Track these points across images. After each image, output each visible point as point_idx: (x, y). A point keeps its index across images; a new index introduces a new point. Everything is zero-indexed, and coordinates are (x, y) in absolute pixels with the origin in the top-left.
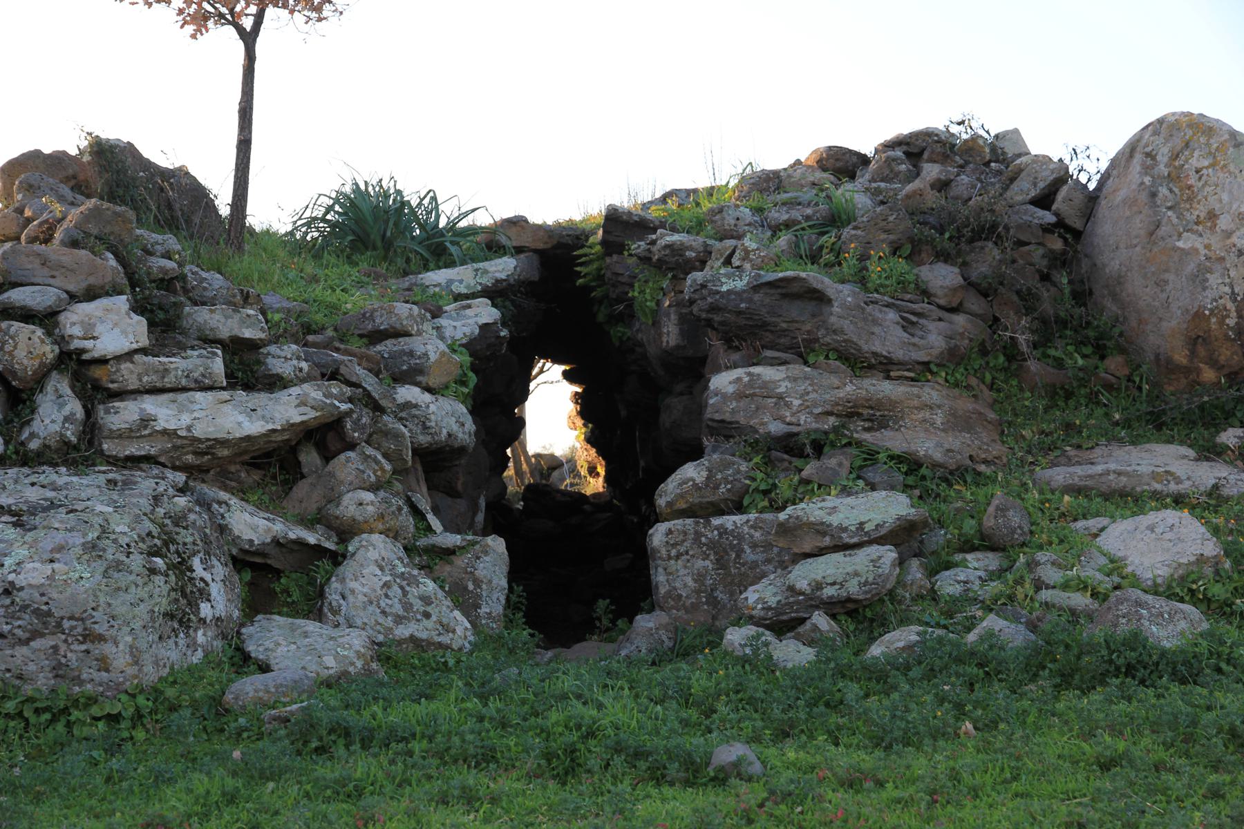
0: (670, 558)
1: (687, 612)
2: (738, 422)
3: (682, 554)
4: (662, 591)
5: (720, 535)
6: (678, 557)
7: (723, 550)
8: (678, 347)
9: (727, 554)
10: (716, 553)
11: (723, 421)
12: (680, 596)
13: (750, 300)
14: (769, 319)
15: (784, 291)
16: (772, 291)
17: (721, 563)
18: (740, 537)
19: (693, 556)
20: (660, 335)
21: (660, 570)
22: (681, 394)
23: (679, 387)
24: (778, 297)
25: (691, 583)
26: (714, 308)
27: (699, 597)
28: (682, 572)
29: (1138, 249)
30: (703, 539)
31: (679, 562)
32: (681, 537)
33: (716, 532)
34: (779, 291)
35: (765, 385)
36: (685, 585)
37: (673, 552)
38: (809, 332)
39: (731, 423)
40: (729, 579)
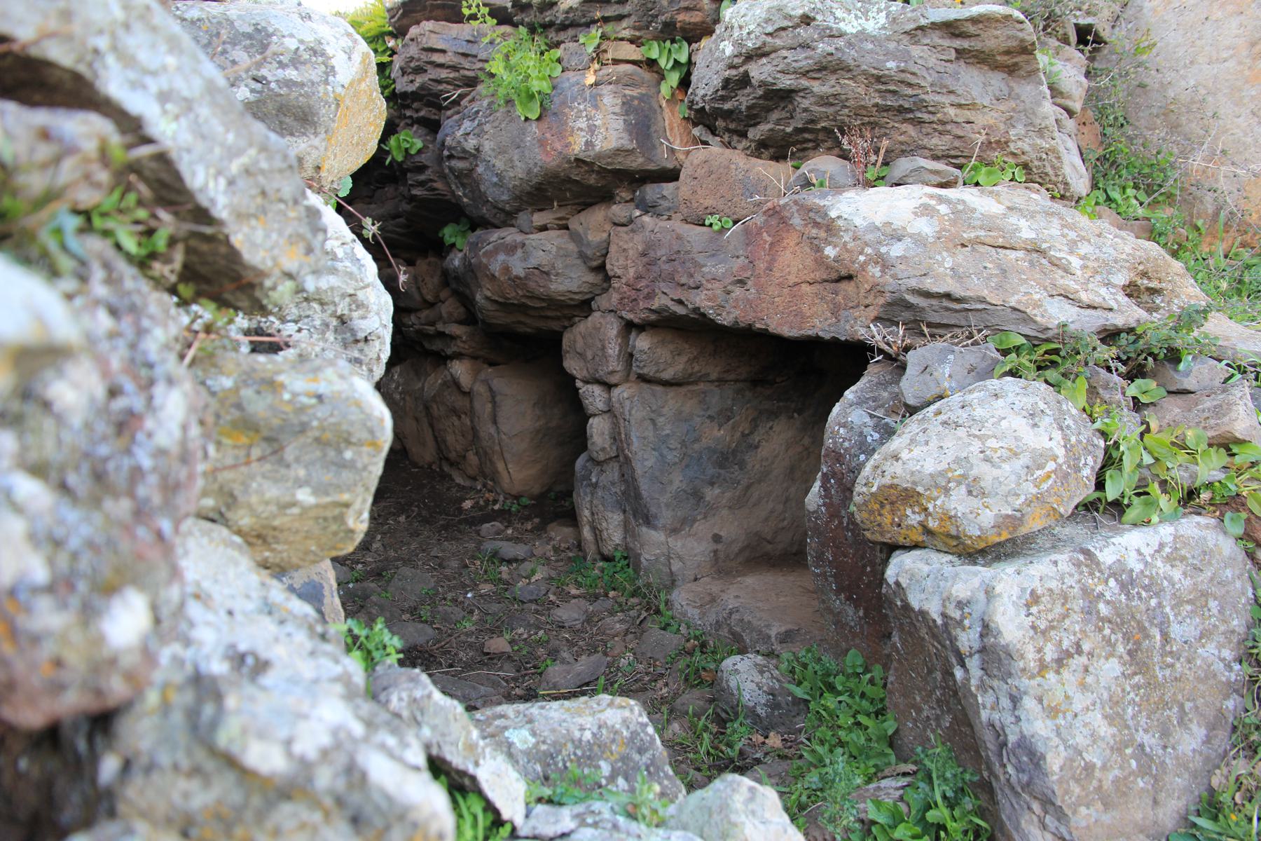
0: (1043, 667)
1: (1107, 806)
2: (982, 300)
3: (1069, 655)
4: (1054, 762)
5: (1123, 587)
6: (1060, 662)
7: (1134, 631)
8: (618, 151)
9: (1147, 636)
10: (1127, 637)
11: (948, 296)
12: (1089, 768)
13: (906, 56)
14: (931, 98)
15: (965, 44)
16: (946, 43)
17: (1136, 659)
18: (1153, 587)
19: (1091, 654)
20: (562, 132)
21: (1029, 703)
22: (544, 228)
23: (539, 218)
24: (953, 55)
25: (1105, 730)
26: (825, 68)
27: (1125, 760)
28: (1080, 701)
29: (1231, 64)
30: (1103, 609)
31: (1066, 674)
32: (1058, 610)
33: (1112, 583)
34: (958, 43)
35: (989, 224)
36: (1094, 737)
37: (1050, 653)
38: (989, 128)
39: (958, 300)
40: (1155, 697)
